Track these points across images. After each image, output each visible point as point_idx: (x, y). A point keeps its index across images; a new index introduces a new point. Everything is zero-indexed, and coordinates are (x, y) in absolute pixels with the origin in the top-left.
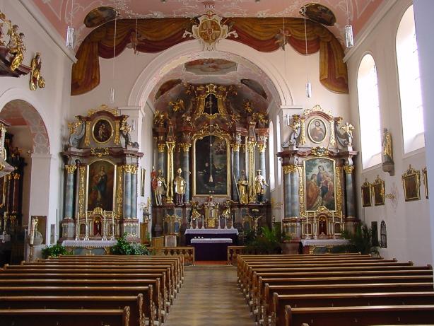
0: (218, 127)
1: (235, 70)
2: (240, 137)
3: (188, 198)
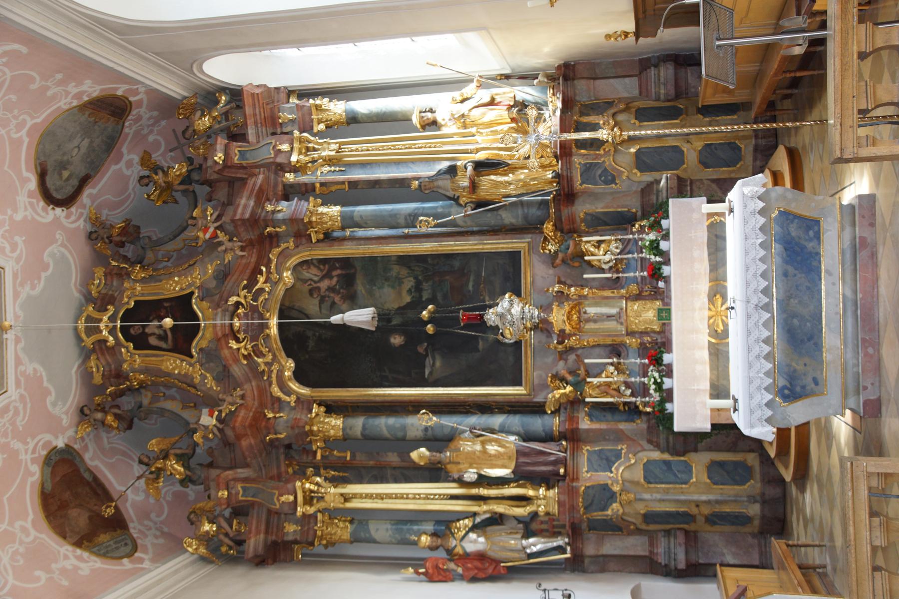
0: (242, 296)
2: (283, 205)
3: (537, 424)
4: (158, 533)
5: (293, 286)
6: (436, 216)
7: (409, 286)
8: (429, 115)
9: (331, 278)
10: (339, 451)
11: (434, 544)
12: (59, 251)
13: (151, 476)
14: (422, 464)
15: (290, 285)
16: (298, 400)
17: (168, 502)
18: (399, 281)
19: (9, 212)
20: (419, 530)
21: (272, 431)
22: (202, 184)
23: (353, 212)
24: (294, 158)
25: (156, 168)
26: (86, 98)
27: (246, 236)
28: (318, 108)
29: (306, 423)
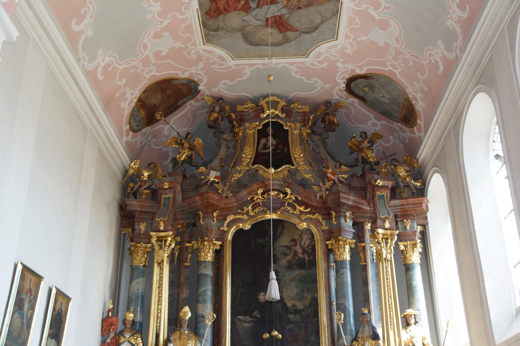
0: (291, 197)
1: (334, 35)
2: (350, 223)
4: (143, 143)
5: (297, 229)
6: (344, 325)
7: (297, 306)
8: (413, 321)
9: (303, 253)
10: (191, 257)
11: (127, 323)
12: (319, 86)
13: (179, 141)
14: (181, 314)
15: (298, 226)
16: (224, 232)
17: (162, 149)
18: (301, 299)
19: (342, 60)
20: (137, 311)
21: (205, 216)
22: (362, 170)
23: (346, 268)
24: (380, 231)
25: (372, 142)
26: (414, 102)
27: (329, 199)
28: (415, 245)
29: (209, 237)
